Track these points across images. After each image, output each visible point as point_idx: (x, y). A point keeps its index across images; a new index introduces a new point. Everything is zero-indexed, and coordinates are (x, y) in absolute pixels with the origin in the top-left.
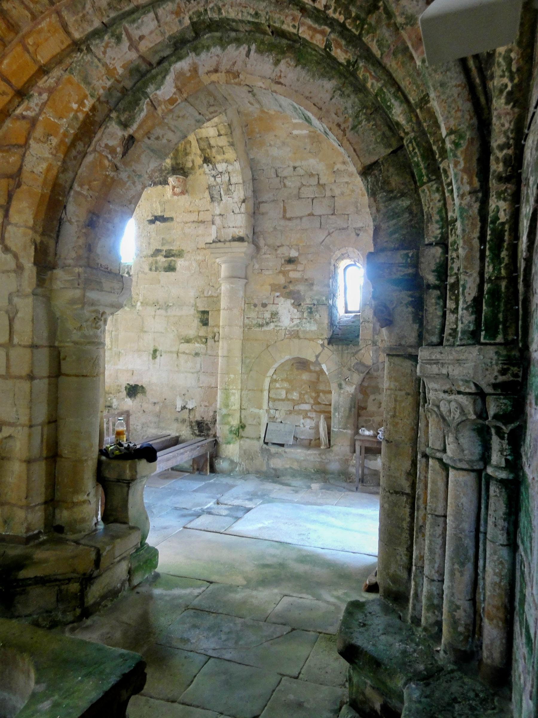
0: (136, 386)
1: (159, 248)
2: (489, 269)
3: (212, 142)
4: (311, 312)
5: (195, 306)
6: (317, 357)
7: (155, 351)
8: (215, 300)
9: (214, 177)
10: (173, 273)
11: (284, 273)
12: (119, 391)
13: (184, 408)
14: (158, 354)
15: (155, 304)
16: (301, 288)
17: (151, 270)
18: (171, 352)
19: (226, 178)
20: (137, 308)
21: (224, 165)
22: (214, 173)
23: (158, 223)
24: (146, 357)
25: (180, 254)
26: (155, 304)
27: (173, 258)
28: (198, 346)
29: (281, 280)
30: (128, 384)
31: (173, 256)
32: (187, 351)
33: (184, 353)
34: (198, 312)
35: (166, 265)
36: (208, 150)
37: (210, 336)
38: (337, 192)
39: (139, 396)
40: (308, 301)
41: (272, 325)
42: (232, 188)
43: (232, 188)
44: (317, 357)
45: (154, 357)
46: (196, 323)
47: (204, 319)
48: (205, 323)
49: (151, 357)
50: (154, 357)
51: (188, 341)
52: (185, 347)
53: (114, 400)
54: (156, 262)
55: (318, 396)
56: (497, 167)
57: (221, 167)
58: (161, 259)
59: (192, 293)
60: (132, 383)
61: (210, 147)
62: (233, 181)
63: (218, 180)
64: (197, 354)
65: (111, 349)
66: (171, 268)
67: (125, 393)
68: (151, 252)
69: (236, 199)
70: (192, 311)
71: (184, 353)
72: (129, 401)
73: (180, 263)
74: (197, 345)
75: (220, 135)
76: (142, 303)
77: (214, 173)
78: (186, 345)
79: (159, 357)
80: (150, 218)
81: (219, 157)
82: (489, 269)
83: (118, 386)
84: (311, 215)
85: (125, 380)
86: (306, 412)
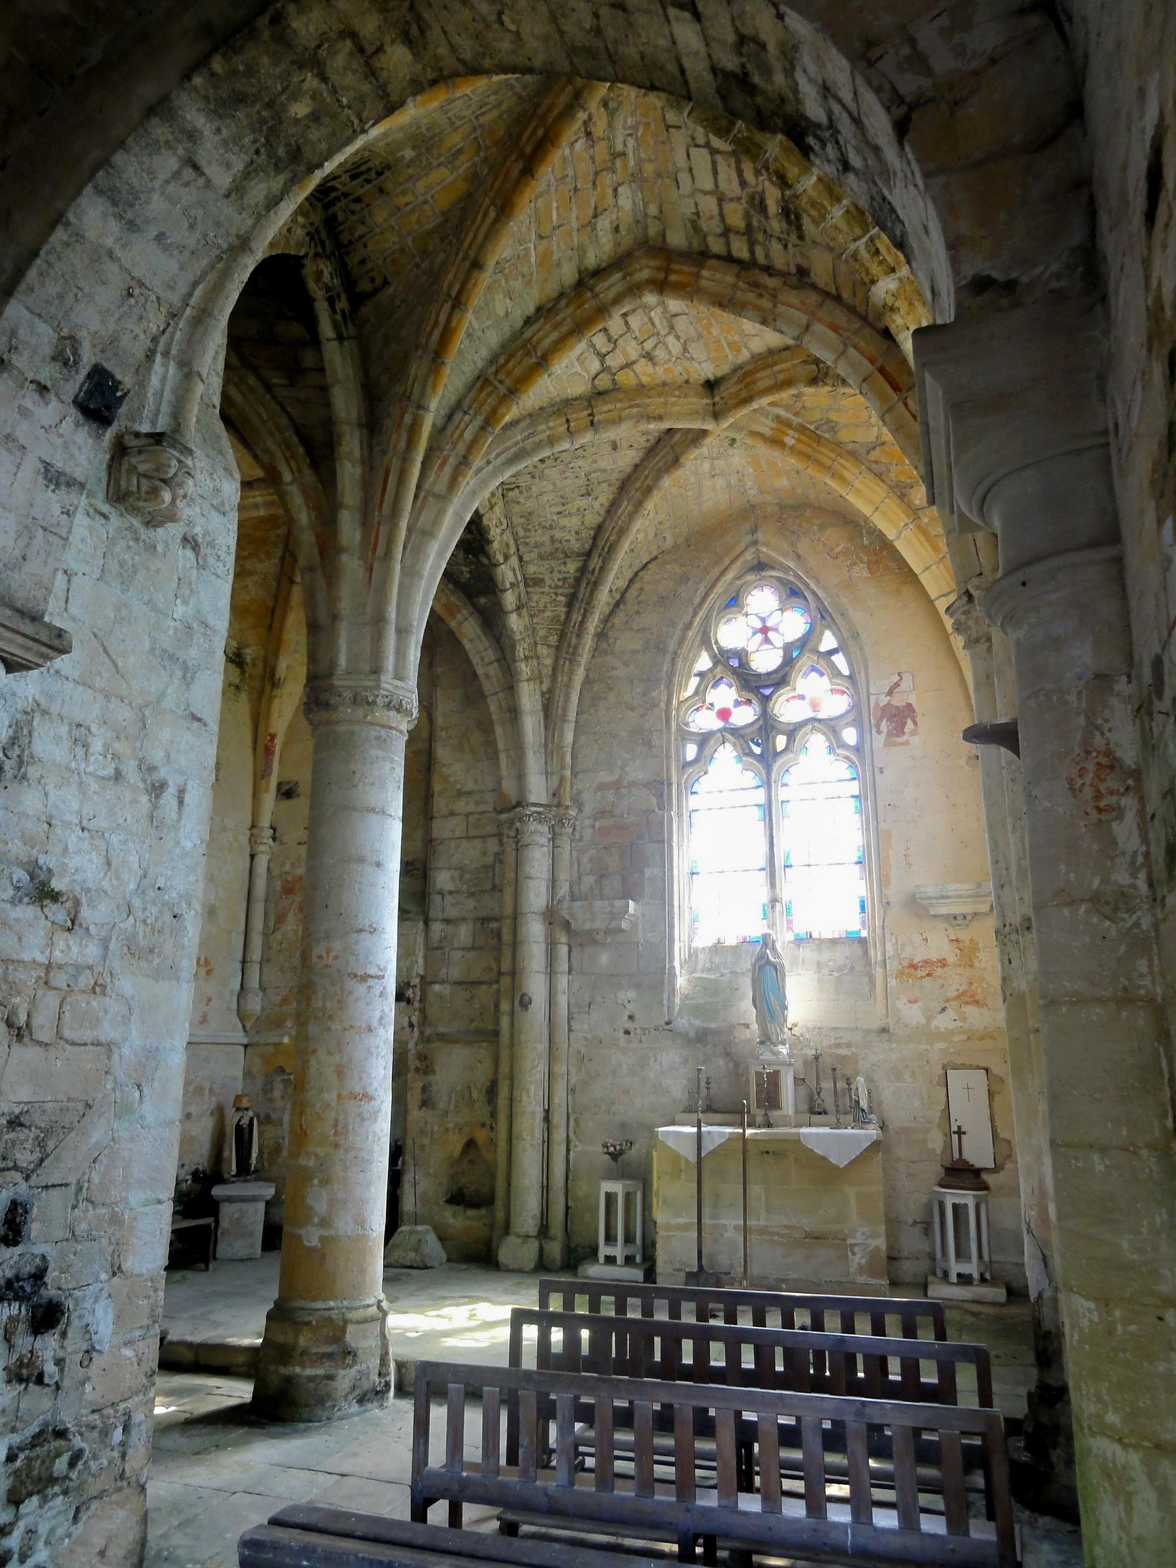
36: (759, 100)
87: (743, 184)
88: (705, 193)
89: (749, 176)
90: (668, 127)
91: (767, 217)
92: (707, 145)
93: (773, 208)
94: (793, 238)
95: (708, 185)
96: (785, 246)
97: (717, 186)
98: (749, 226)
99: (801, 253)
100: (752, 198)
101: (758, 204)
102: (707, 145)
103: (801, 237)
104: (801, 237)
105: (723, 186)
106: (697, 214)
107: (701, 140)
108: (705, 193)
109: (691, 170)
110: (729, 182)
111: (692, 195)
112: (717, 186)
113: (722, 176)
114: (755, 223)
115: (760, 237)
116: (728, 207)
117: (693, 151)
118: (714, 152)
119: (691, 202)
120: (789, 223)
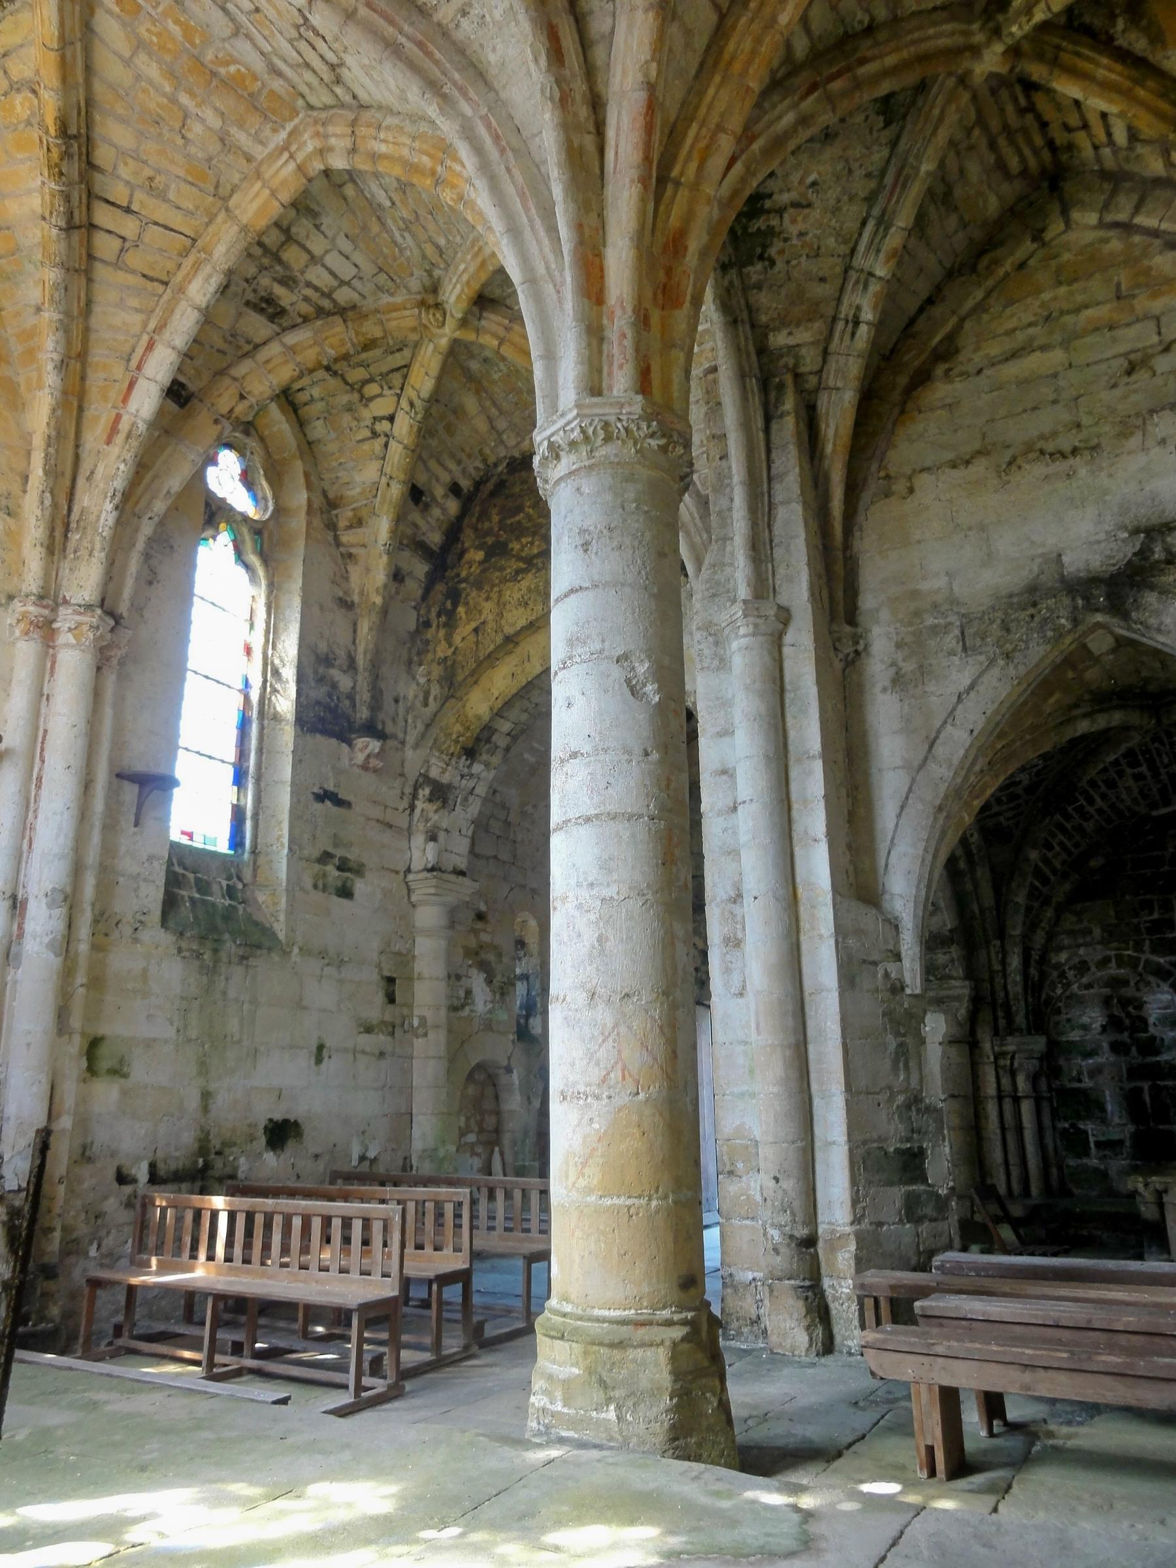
0: (286, 1122)
1: (330, 850)
2: (1030, 1000)
3: (494, 738)
4: (502, 994)
5: (379, 966)
6: (509, 1058)
7: (321, 1048)
8: (405, 959)
9: (462, 776)
10: (344, 902)
11: (475, 932)
12: (252, 1139)
13: (362, 1158)
14: (325, 1053)
15: (322, 954)
16: (491, 957)
17: (315, 886)
18: (346, 1050)
19: (471, 784)
20: (293, 959)
21: (482, 767)
22: (466, 771)
23: (328, 803)
24: (304, 1060)
25: (359, 871)
26: (322, 954)
27: (348, 874)
28: (380, 1040)
29: (472, 943)
30: (271, 1120)
31: (349, 870)
32: (368, 1049)
33: (363, 1052)
34: (383, 977)
35: (339, 884)
37: (398, 1022)
38: (519, 838)
39: (291, 1144)
40: (499, 978)
41: (467, 1009)
42: (471, 798)
43: (471, 798)
44: (509, 1058)
45: (319, 1060)
46: (380, 998)
47: (391, 989)
48: (391, 999)
49: (313, 1061)
50: (319, 1060)
51: (369, 1030)
52: (364, 1040)
53: (242, 1160)
54: (325, 875)
55: (482, 1120)
56: (1035, 956)
57: (477, 768)
58: (331, 870)
59: (376, 944)
60: (278, 1116)
61: (488, 741)
62: (477, 791)
63: (464, 782)
64: (382, 1054)
65: (239, 1042)
66: (345, 892)
67: (263, 1140)
68: (316, 854)
69: (469, 816)
70: (375, 977)
71: (363, 1052)
72: (270, 1157)
73: (360, 887)
74: (382, 1037)
75: (508, 734)
76: (301, 949)
77: (466, 771)
78: (366, 1036)
79: (326, 1060)
80: (316, 790)
81: (485, 757)
82: (1030, 1000)
83: (250, 1125)
84: (495, 857)
85: (266, 1111)
86: (472, 1145)
87: (309, 284)
88: (327, 252)
89: (309, 292)
90: (381, 270)
91: (275, 279)
92: (348, 284)
93: (279, 290)
94: (250, 296)
95: (329, 260)
96: (247, 281)
97: (324, 265)
98: (280, 261)
99: (236, 295)
100: (295, 281)
101: (288, 281)
102: (348, 284)
103: (248, 303)
104: (248, 303)
105: (320, 270)
106: (317, 227)
107: (355, 282)
108: (327, 252)
109: (347, 258)
110: (318, 276)
111: (333, 239)
112: (324, 265)
113: (326, 276)
114: (278, 268)
115: (266, 261)
116: (305, 257)
117: (354, 271)
118: (343, 283)
119: (330, 234)
120: (262, 299)
